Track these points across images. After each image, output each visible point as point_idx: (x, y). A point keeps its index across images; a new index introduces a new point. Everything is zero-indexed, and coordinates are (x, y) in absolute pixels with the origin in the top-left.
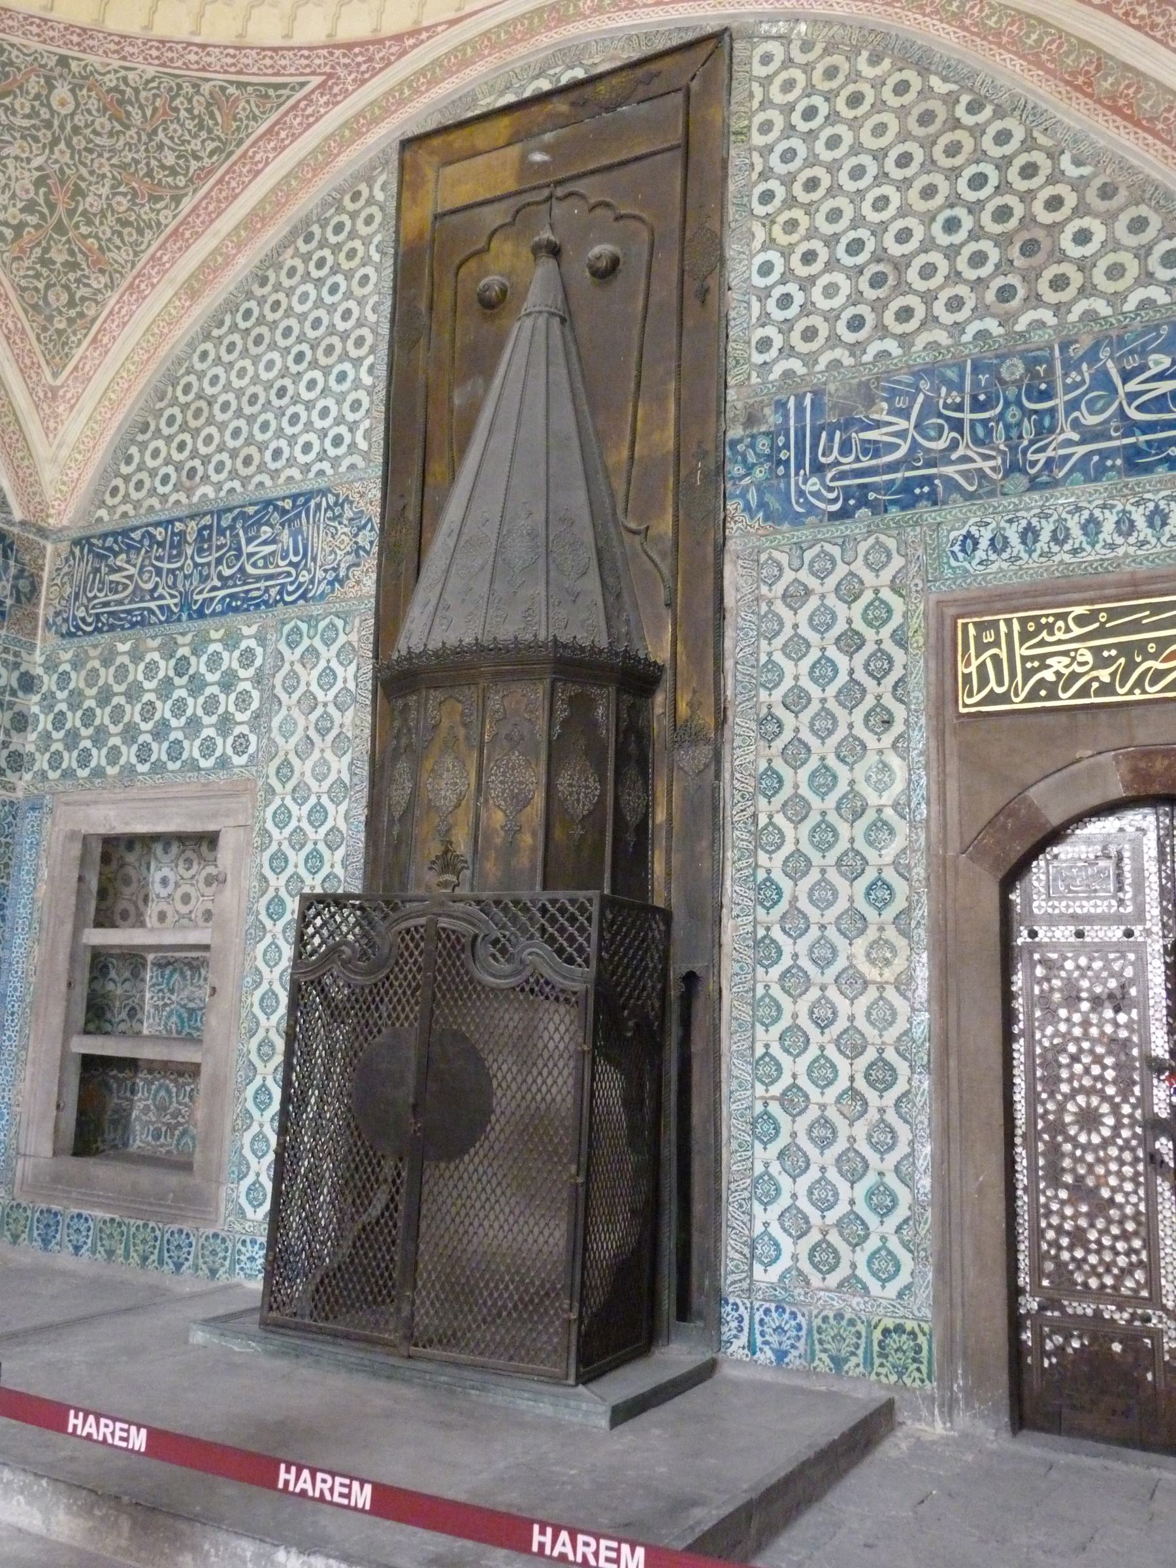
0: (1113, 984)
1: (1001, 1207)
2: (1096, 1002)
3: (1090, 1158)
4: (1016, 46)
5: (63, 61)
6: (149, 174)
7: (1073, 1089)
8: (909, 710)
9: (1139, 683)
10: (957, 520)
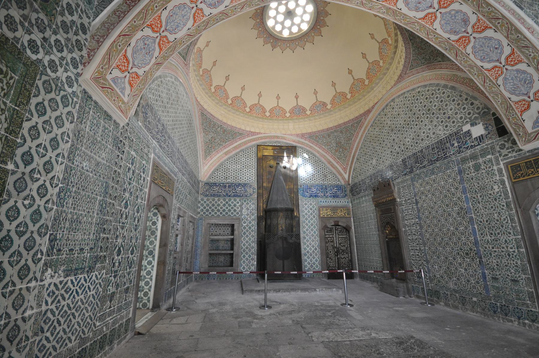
10: (320, 199)
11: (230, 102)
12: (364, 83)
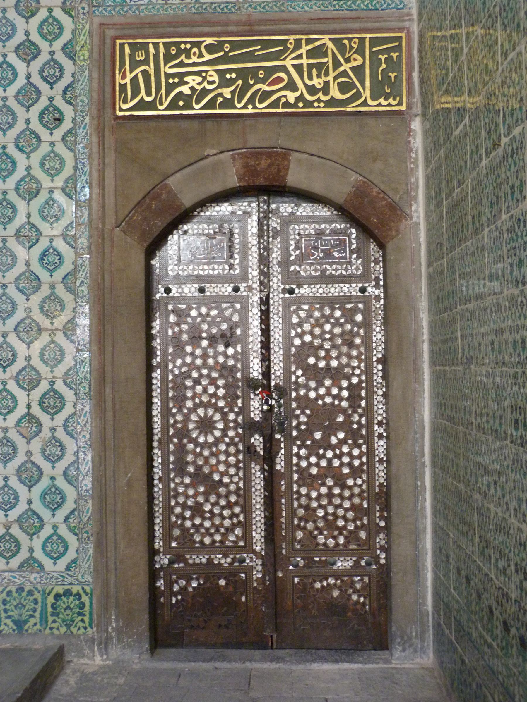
0: (224, 326)
1: (144, 494)
2: (213, 340)
3: (206, 453)
7: (195, 404)
8: (75, 110)
9: (251, 100)
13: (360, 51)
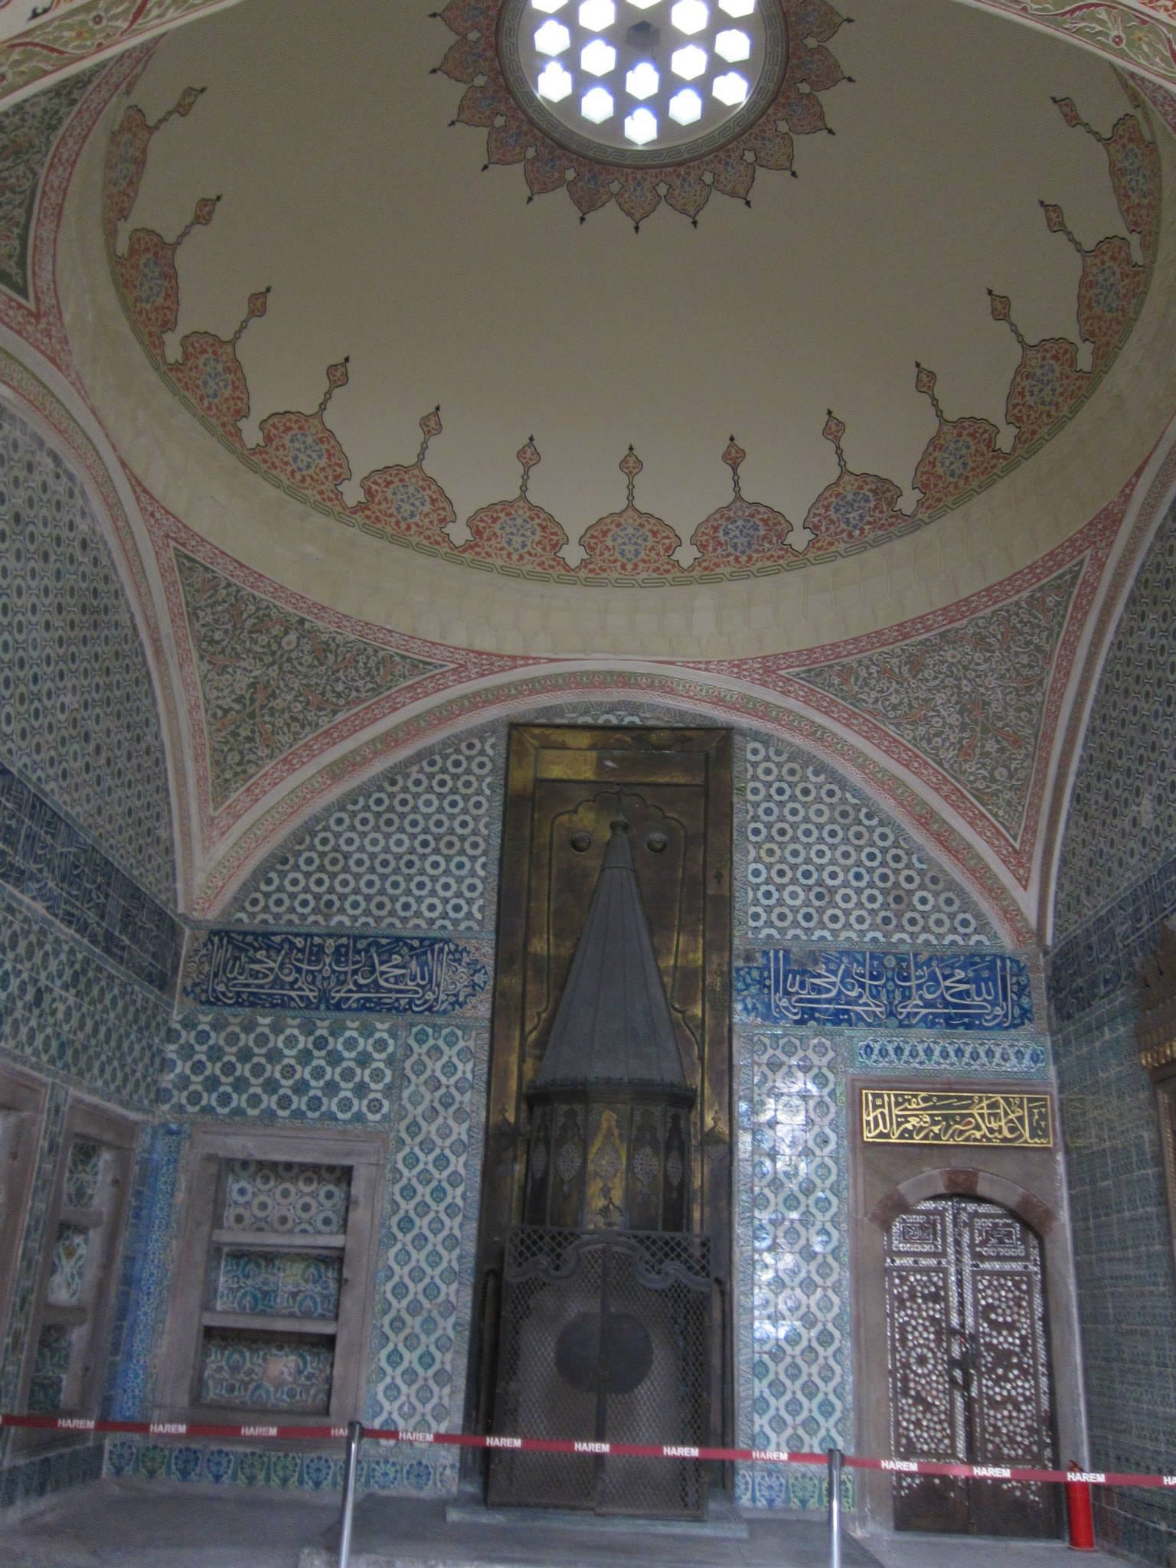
4: (891, 792)
5: (302, 621)
6: (323, 694)
10: (860, 1036)
11: (353, 494)
12: (1073, 362)
13: (1021, 1106)
